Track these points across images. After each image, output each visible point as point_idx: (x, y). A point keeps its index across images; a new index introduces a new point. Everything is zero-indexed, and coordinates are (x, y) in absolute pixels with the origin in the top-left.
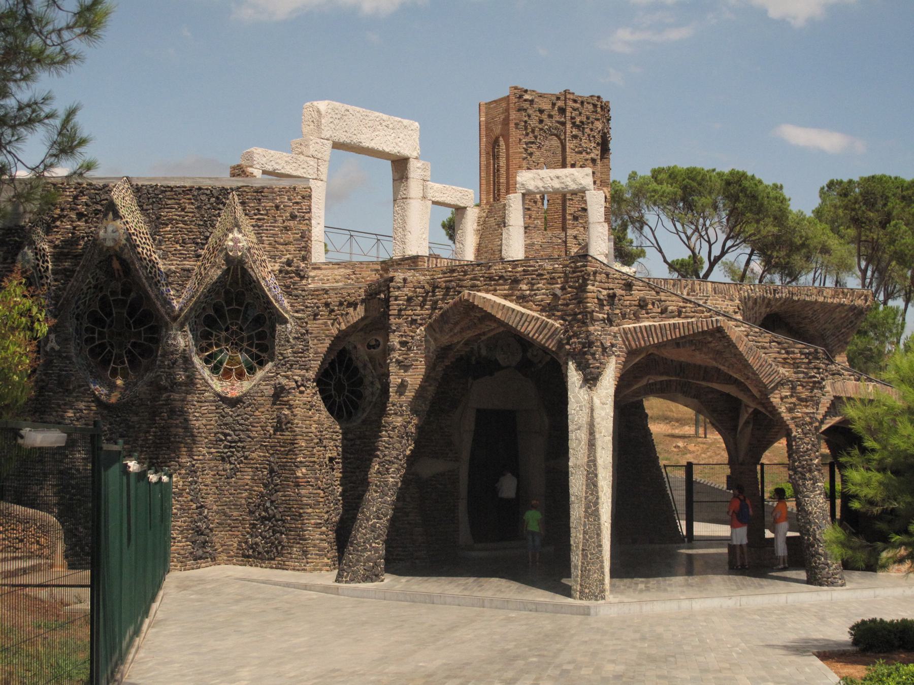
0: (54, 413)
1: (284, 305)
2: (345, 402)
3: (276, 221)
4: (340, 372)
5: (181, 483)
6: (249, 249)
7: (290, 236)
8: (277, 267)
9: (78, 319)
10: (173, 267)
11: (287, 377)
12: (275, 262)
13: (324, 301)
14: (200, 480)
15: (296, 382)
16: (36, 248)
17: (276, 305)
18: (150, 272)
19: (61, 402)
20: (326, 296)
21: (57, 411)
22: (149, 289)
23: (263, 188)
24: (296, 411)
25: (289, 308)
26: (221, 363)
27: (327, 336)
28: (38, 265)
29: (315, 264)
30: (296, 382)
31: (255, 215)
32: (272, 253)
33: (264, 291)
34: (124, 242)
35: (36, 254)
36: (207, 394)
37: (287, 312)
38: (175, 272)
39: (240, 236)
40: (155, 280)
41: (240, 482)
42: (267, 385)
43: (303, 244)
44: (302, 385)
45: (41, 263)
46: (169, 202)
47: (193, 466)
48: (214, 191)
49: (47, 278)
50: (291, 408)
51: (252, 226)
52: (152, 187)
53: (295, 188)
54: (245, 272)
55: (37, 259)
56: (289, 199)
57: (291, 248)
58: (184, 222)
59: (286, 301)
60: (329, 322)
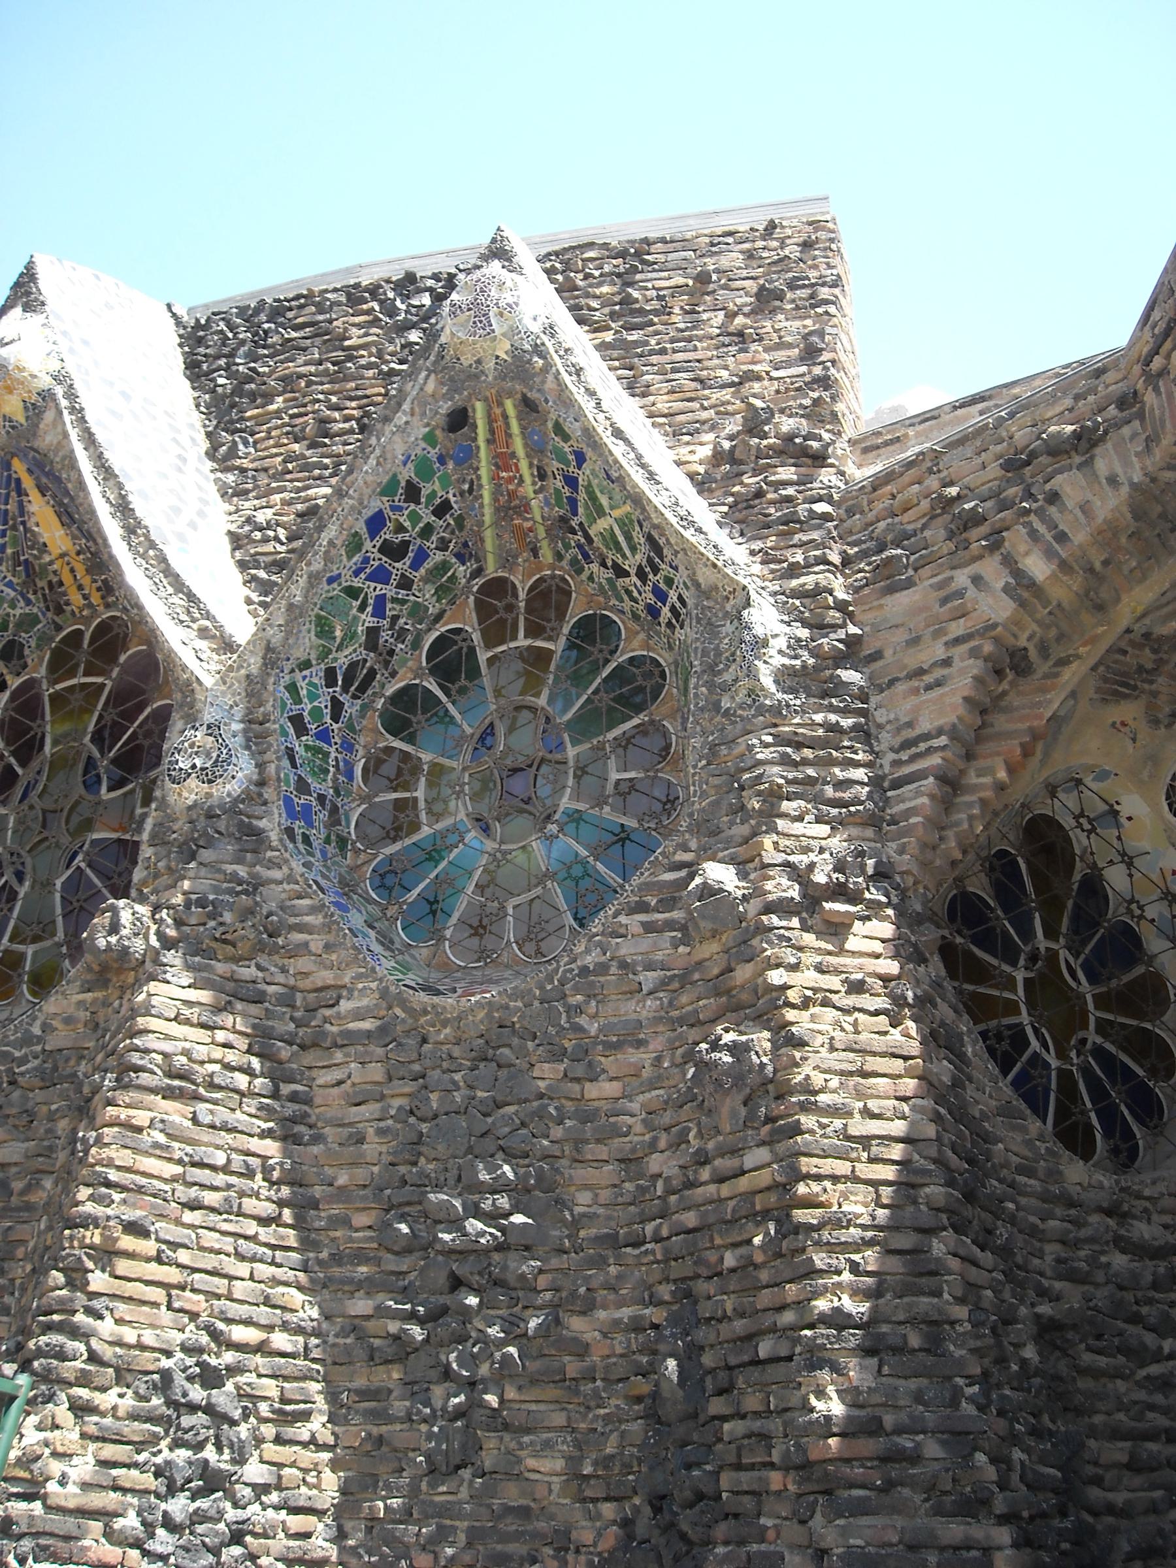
2: (1086, 1071)
4: (1051, 933)
5: (83, 1467)
11: (748, 864)
13: (925, 504)
14: (255, 1471)
15: (800, 875)
20: (933, 483)
23: (646, 241)
24: (800, 1021)
26: (448, 884)
27: (957, 641)
30: (800, 875)
34: (45, 382)
41: (511, 1494)
42: (649, 928)
44: (839, 892)
47: (210, 1378)
50: (766, 1007)
52: (242, 310)
53: (771, 226)
60: (962, 578)
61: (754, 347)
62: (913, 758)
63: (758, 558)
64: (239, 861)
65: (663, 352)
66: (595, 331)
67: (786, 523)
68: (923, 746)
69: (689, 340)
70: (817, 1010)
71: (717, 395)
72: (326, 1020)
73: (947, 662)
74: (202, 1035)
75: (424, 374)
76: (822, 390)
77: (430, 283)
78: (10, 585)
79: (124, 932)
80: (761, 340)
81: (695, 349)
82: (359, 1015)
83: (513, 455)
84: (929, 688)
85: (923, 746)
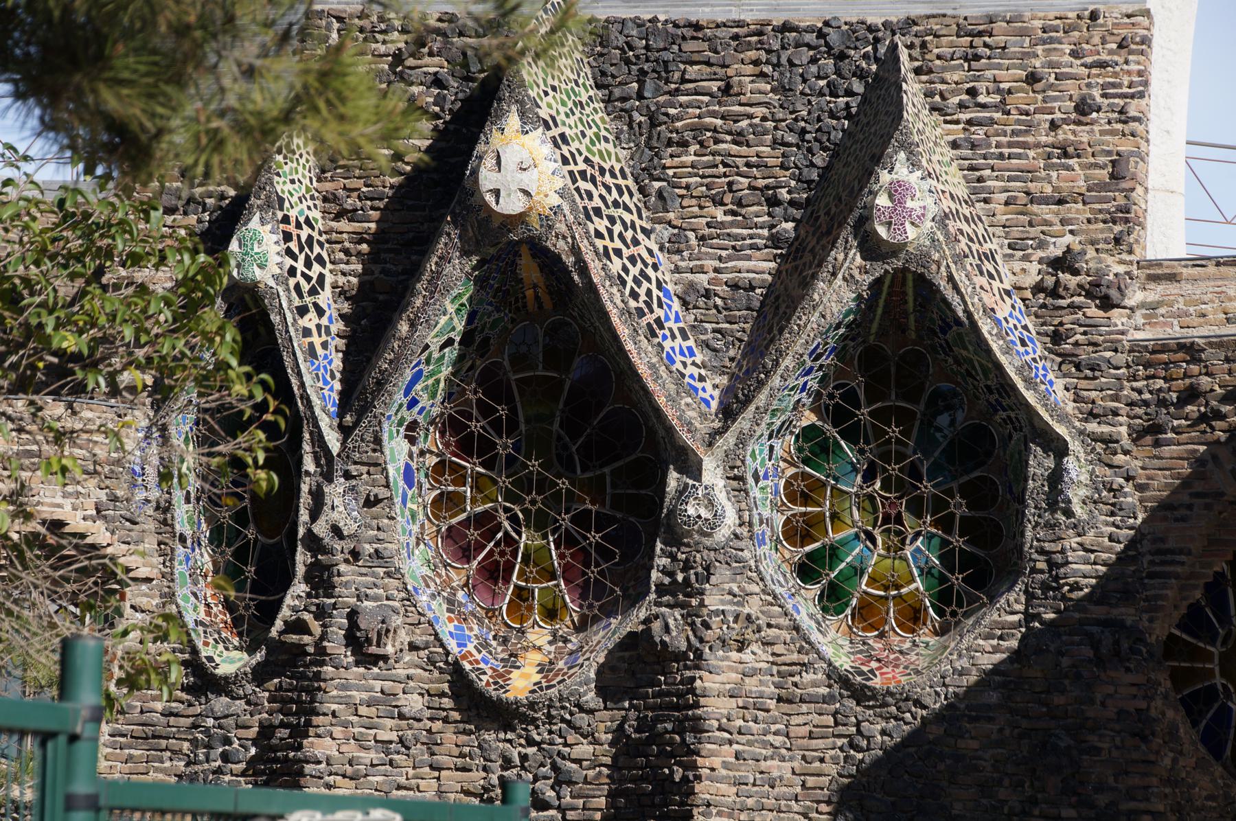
0: (338, 731)
1: (1050, 394)
3: (1030, 127)
6: (942, 220)
7: (1077, 177)
8: (1033, 273)
9: (412, 440)
10: (702, 280)
12: (1026, 258)
16: (286, 219)
17: (1030, 397)
18: (634, 295)
19: (358, 696)
21: (345, 725)
22: (629, 346)
25: (1070, 407)
27: (1198, 495)
28: (292, 271)
29: (1158, 263)
30: (1095, 645)
31: (962, 106)
32: (1016, 232)
33: (989, 351)
34: (555, 200)
35: (287, 237)
36: (808, 677)
37: (1063, 418)
38: (707, 294)
39: (914, 178)
40: (650, 318)
43: (1121, 201)
45: (300, 266)
46: (692, 71)
48: (833, 37)
49: (320, 312)
51: (955, 145)
53: (1094, 16)
54: (925, 287)
55: (289, 252)
56: (1075, 54)
57: (1075, 210)
58: (739, 138)
59: (1059, 384)
61: (1072, 162)
62: (1163, 563)
63: (1070, 395)
64: (734, 581)
65: (1001, 156)
66: (946, 122)
67: (1093, 370)
68: (1169, 557)
69: (1025, 145)
70: (1103, 731)
71: (1045, 212)
72: (795, 685)
73: (1190, 507)
74: (733, 702)
75: (854, 251)
76: (1123, 221)
77: (810, 38)
78: (490, 304)
79: (674, 634)
80: (1079, 156)
81: (1027, 157)
82: (815, 684)
83: (905, 293)
84: (1176, 520)
85: (1169, 557)
